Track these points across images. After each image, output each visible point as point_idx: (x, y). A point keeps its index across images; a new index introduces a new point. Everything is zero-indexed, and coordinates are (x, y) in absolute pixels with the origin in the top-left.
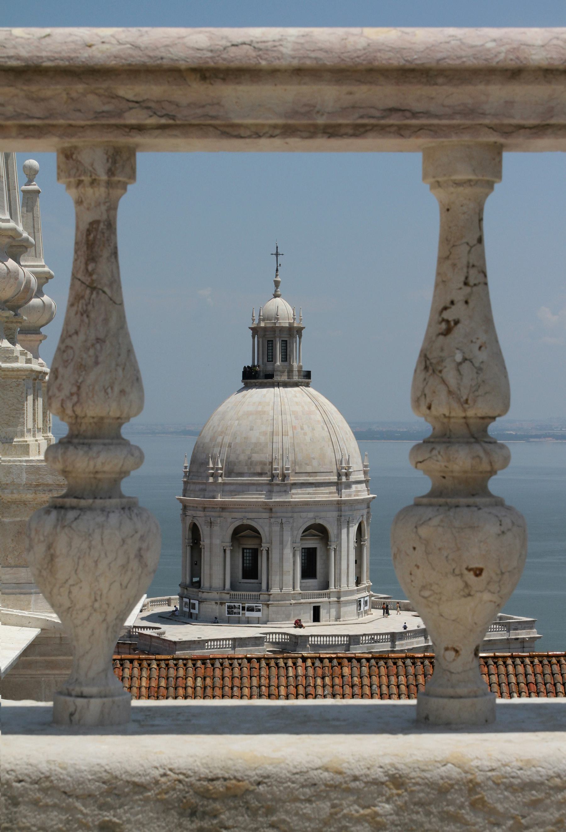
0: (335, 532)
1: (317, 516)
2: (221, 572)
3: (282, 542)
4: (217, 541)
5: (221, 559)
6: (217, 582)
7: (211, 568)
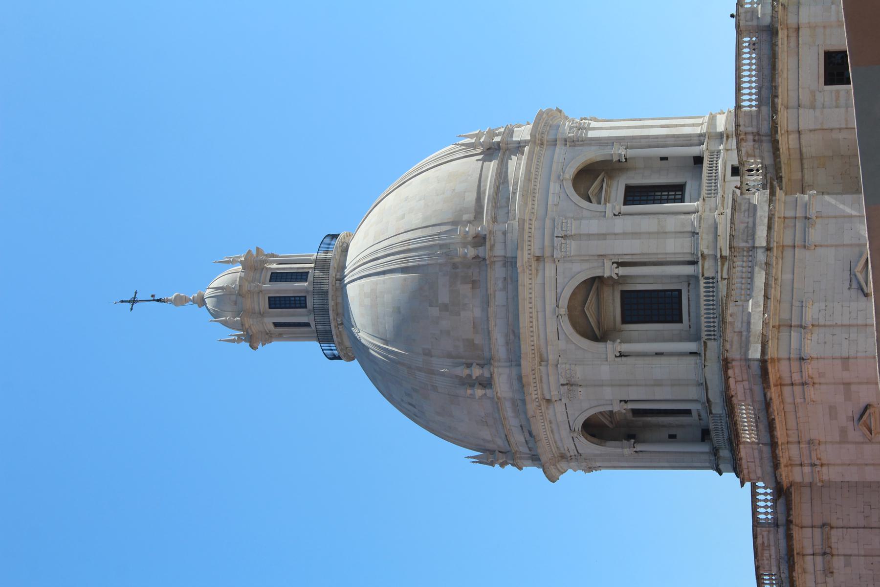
0: (594, 148)
1: (559, 177)
2: (663, 360)
3: (603, 236)
4: (605, 371)
5: (640, 361)
6: (686, 368)
7: (658, 383)
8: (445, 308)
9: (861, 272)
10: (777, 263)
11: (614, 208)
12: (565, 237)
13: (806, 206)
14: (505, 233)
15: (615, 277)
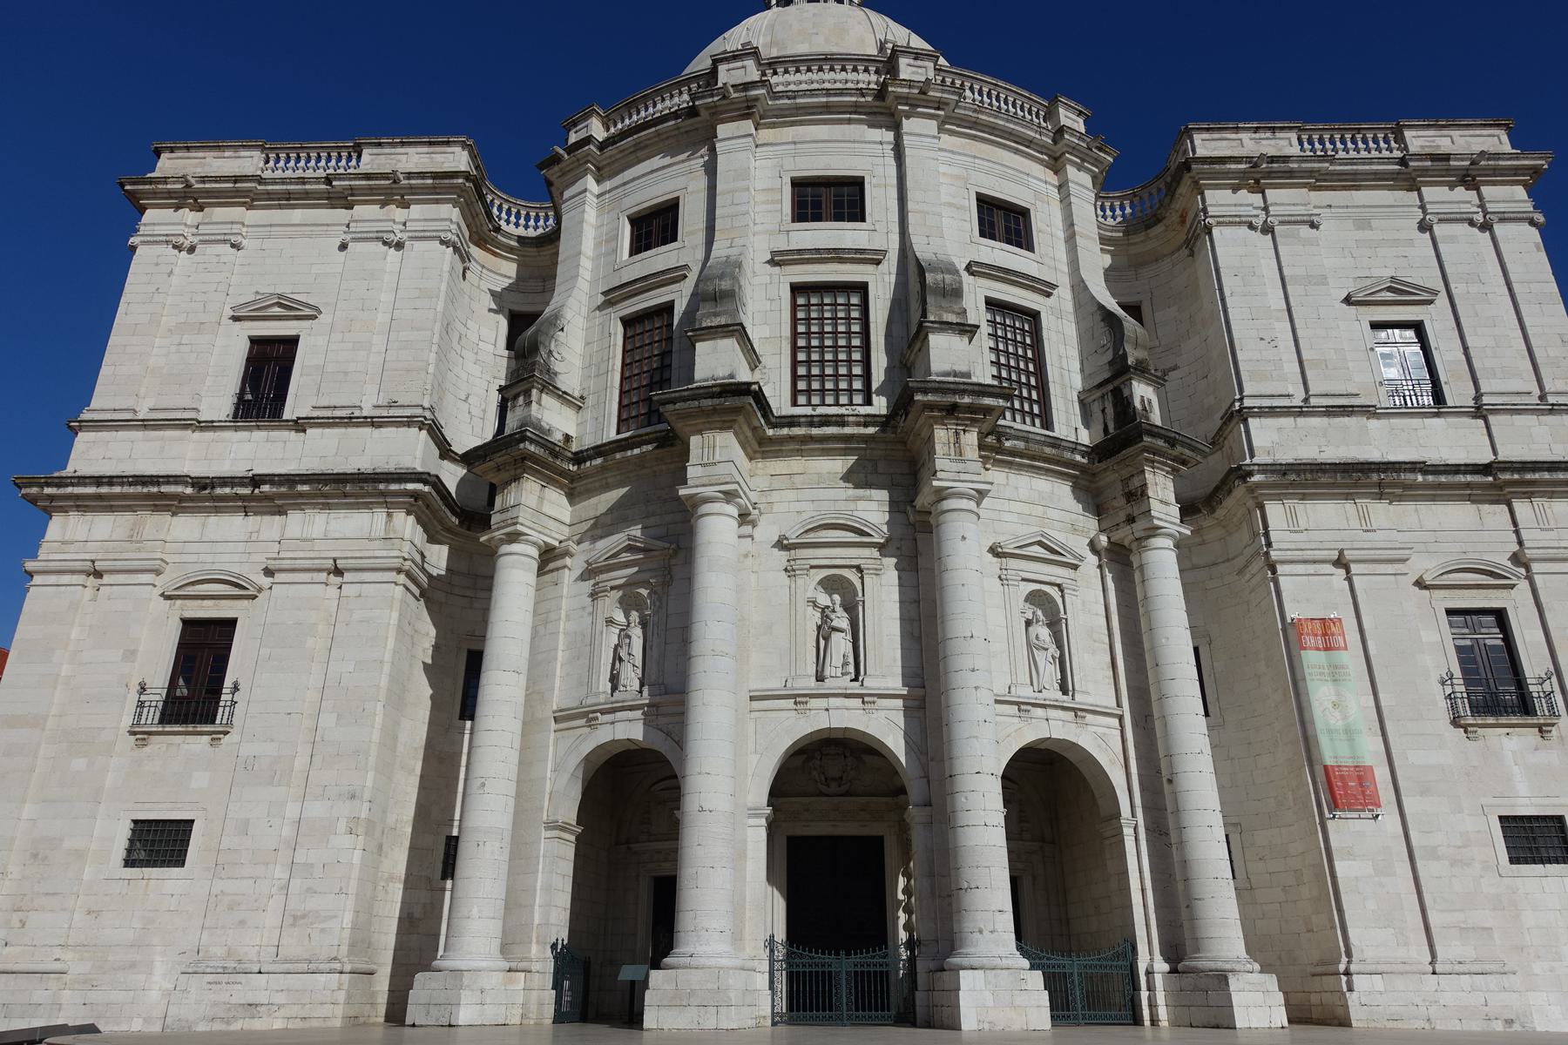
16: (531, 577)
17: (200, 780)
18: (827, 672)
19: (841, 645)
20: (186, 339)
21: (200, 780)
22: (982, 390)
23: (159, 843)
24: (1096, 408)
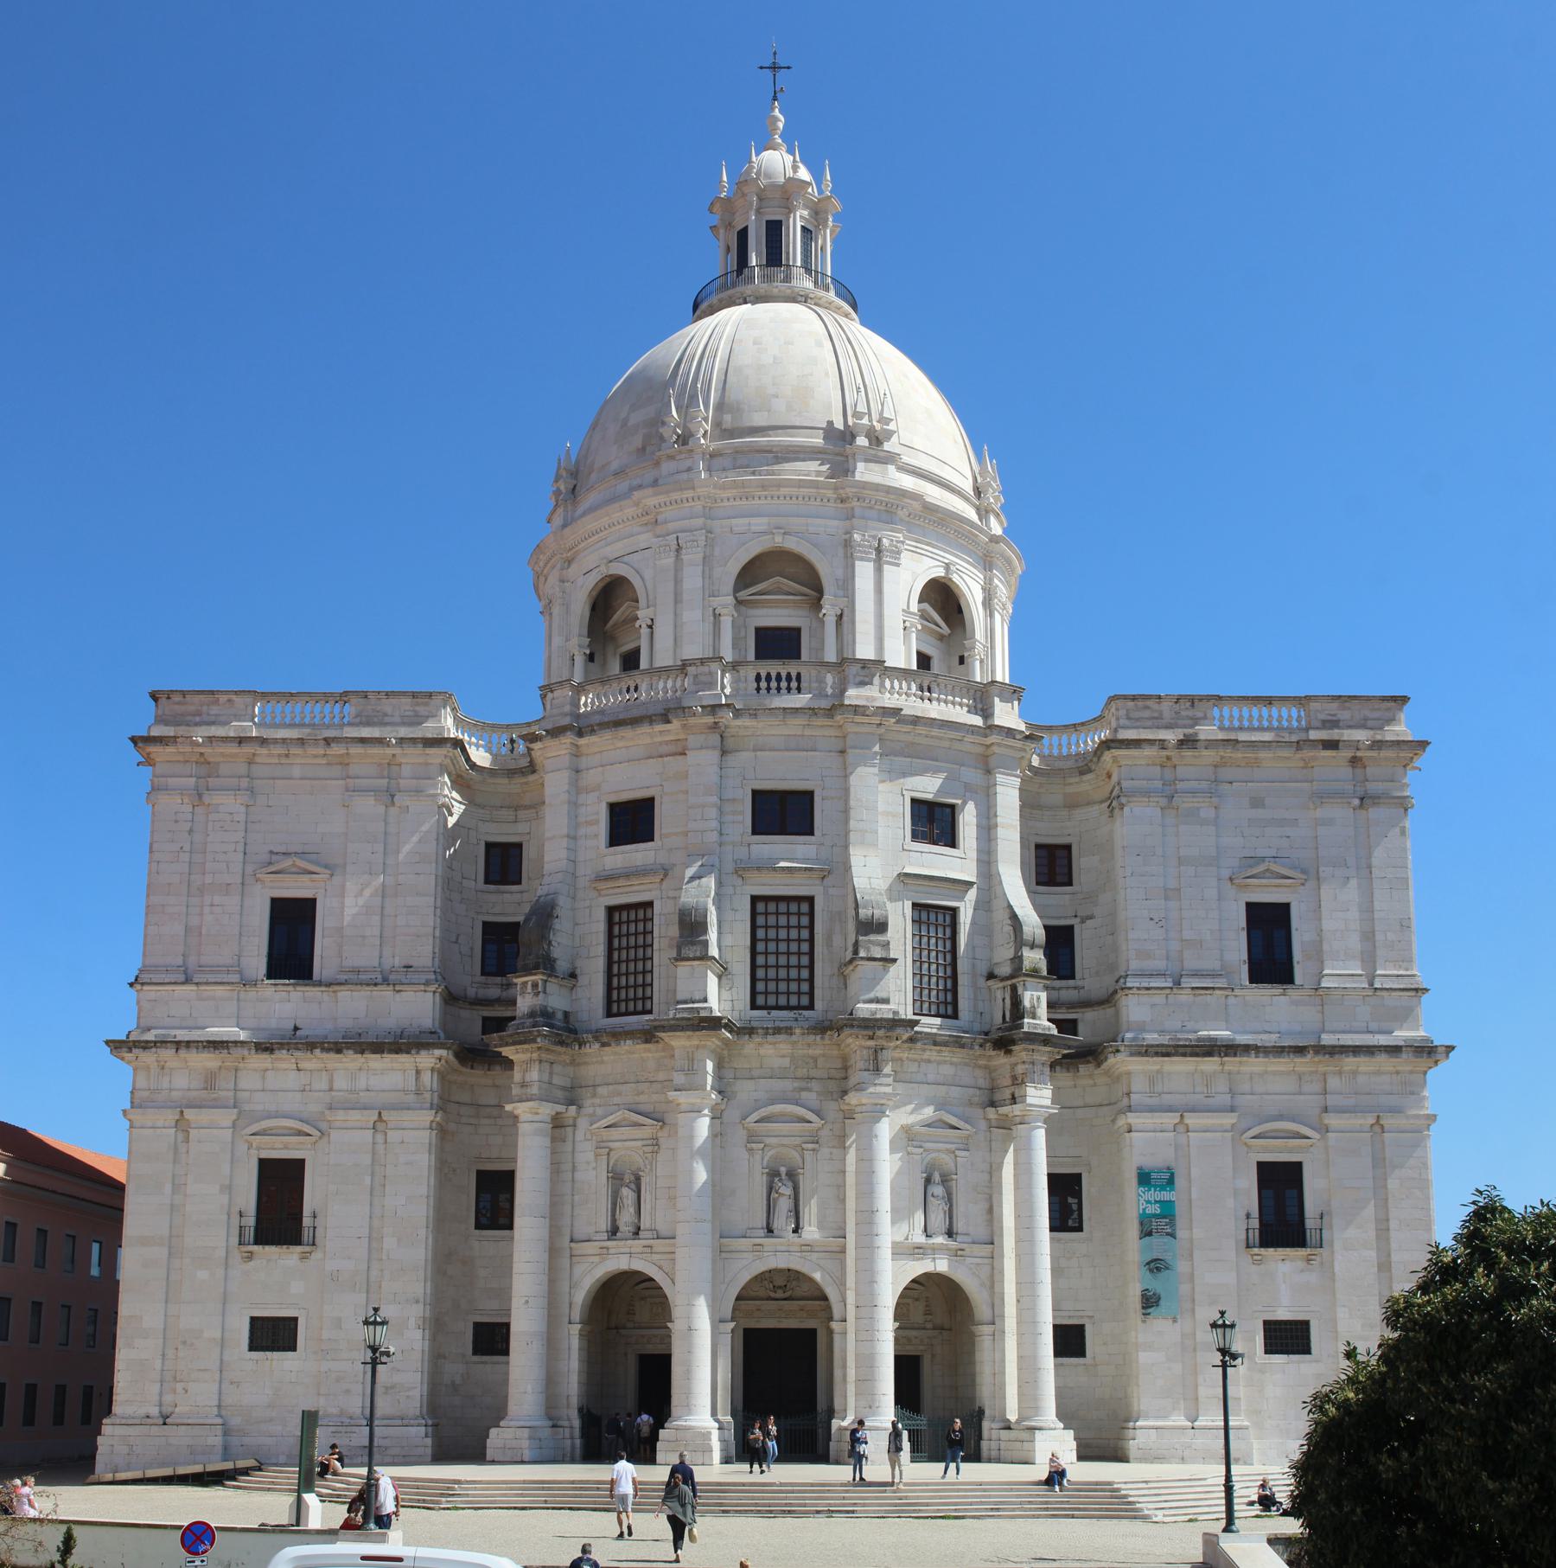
0: (840, 573)
8: (625, 423)
9: (294, 865)
10: (315, 756)
11: (724, 606)
12: (679, 549)
13: (418, 791)
14: (689, 469)
15: (637, 624)
16: (547, 1142)
17: (297, 1287)
18: (776, 1225)
19: (784, 1205)
20: (217, 900)
21: (297, 1287)
22: (895, 1023)
23: (273, 1334)
24: (999, 995)
